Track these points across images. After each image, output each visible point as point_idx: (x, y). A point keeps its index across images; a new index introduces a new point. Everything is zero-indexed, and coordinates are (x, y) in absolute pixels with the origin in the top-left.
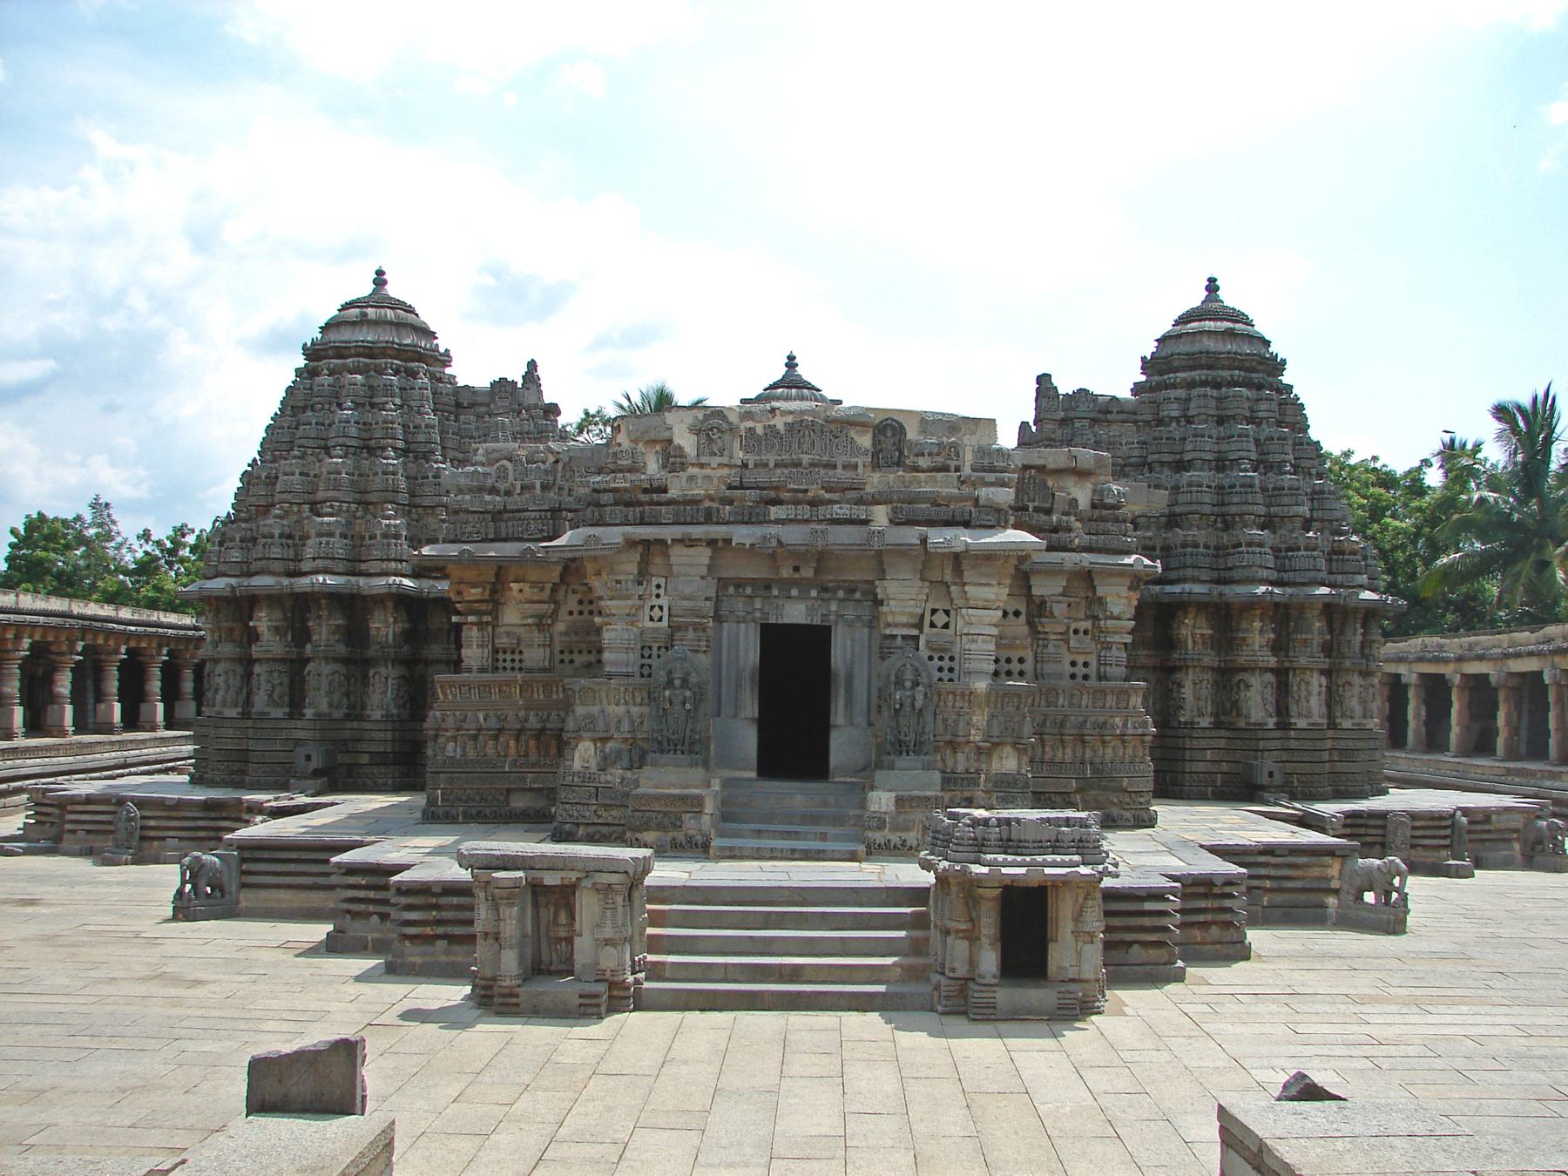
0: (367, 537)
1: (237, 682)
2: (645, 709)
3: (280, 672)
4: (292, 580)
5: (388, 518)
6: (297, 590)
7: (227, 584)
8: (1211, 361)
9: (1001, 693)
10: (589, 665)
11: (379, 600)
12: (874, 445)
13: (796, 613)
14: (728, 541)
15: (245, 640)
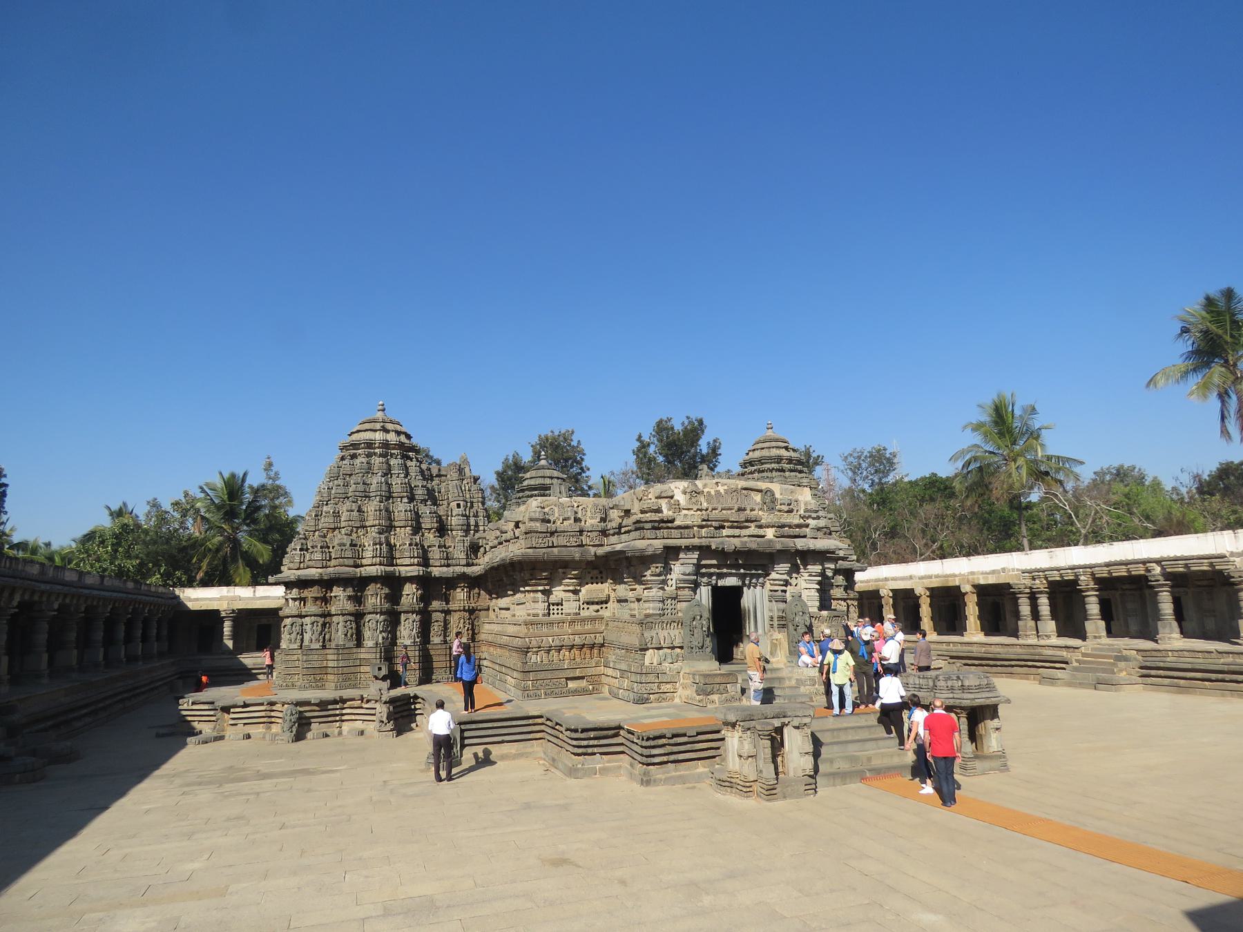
0: (398, 546)
1: (319, 628)
2: (676, 632)
3: (351, 621)
4: (361, 569)
5: (412, 535)
6: (364, 575)
7: (316, 573)
8: (779, 460)
9: (832, 616)
10: (598, 611)
11: (410, 579)
12: (762, 500)
13: (732, 581)
14: (709, 547)
15: (323, 604)
